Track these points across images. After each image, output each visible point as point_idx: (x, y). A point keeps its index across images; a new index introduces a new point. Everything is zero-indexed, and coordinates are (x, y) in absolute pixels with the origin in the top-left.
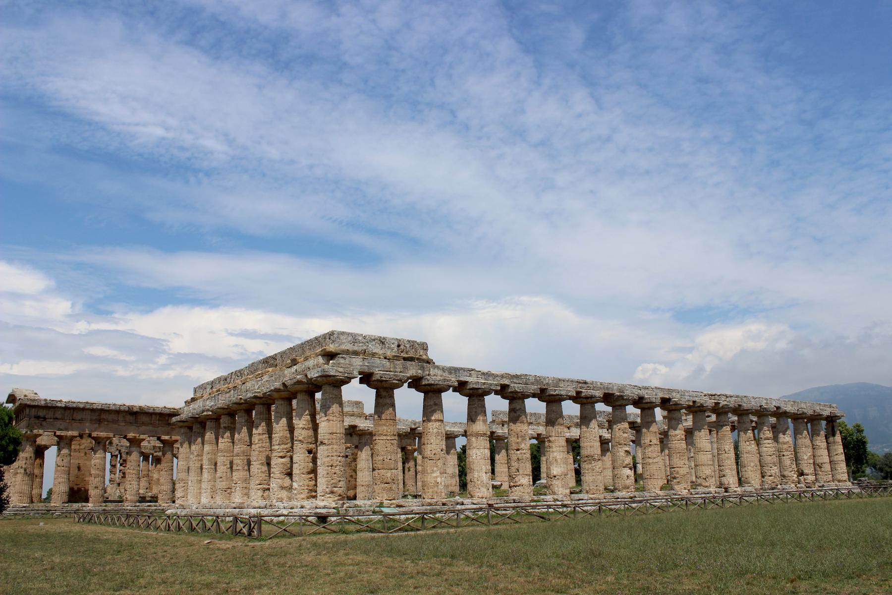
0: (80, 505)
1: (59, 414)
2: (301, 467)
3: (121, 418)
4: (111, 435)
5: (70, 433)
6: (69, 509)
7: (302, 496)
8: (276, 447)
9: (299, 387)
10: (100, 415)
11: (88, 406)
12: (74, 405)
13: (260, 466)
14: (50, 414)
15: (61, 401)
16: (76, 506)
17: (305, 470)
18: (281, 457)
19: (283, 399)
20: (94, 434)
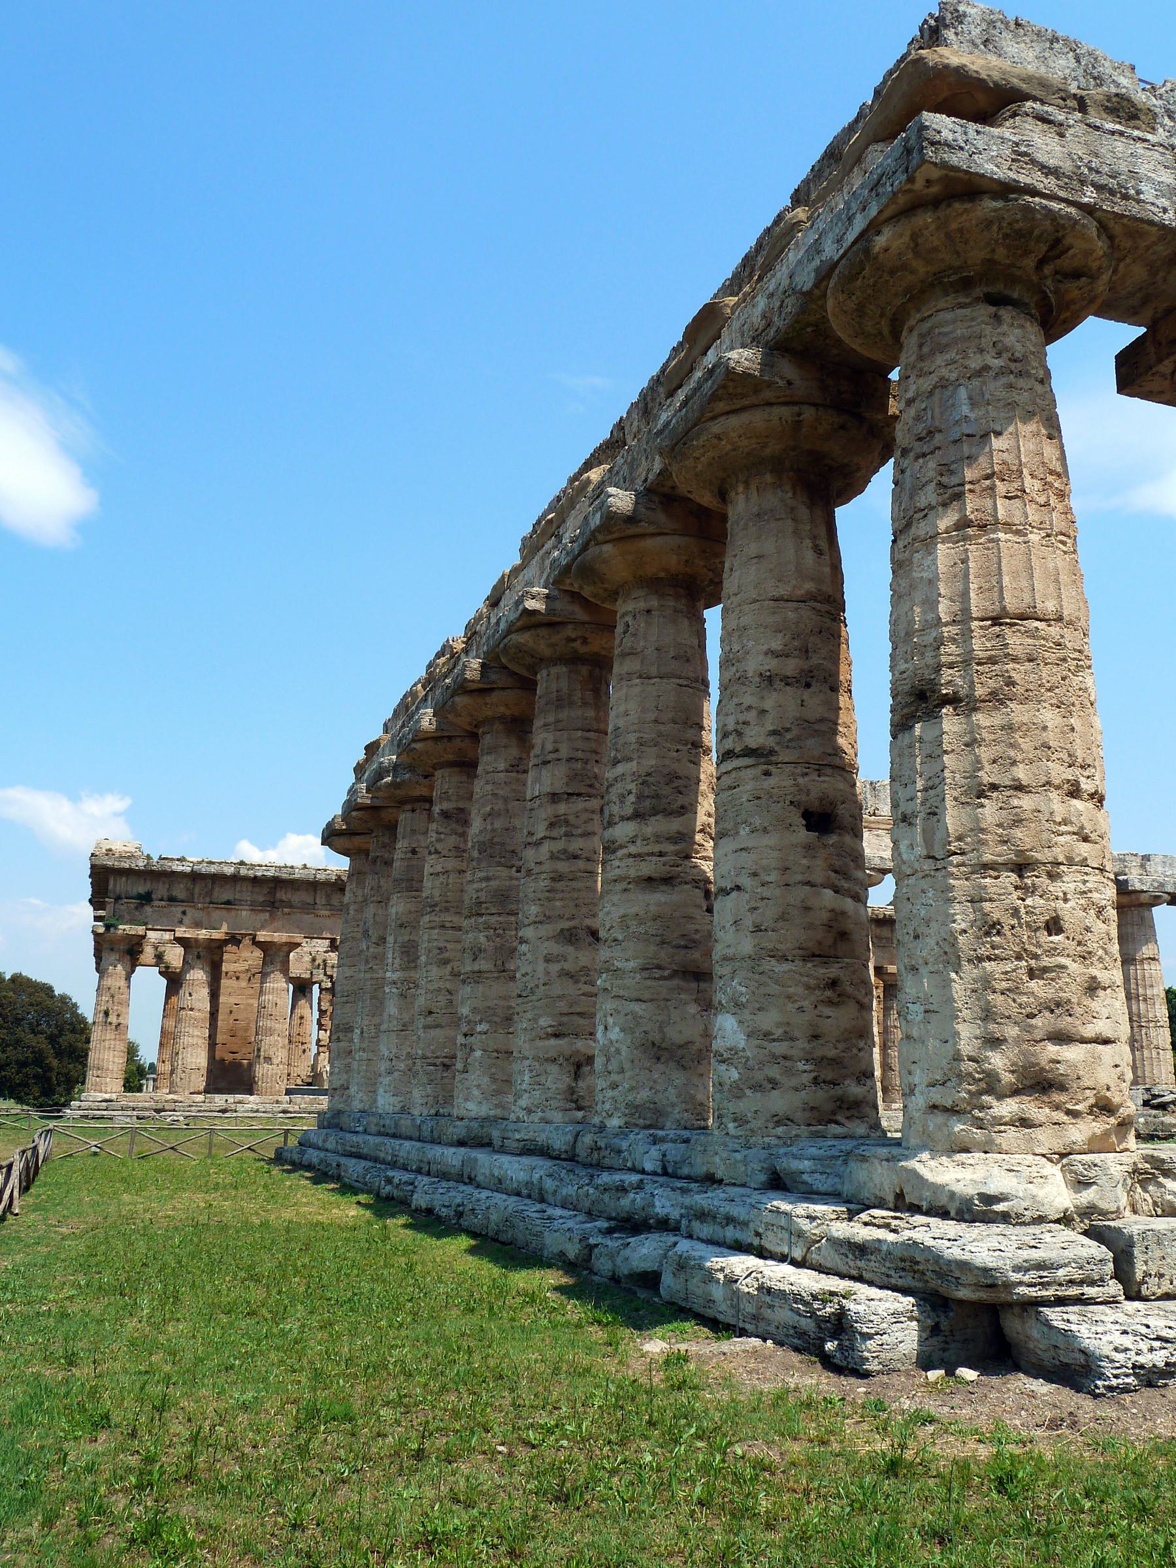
0: (231, 1098)
1: (179, 891)
2: (769, 913)
3: (321, 900)
4: (298, 937)
5: (203, 934)
6: (205, 1107)
7: (778, 1101)
8: (623, 831)
9: (734, 429)
10: (272, 892)
11: (243, 871)
12: (213, 869)
13: (555, 948)
14: (161, 890)
15: (182, 860)
16: (220, 1100)
17: (792, 937)
18: (650, 881)
19: (652, 584)
20: (262, 936)
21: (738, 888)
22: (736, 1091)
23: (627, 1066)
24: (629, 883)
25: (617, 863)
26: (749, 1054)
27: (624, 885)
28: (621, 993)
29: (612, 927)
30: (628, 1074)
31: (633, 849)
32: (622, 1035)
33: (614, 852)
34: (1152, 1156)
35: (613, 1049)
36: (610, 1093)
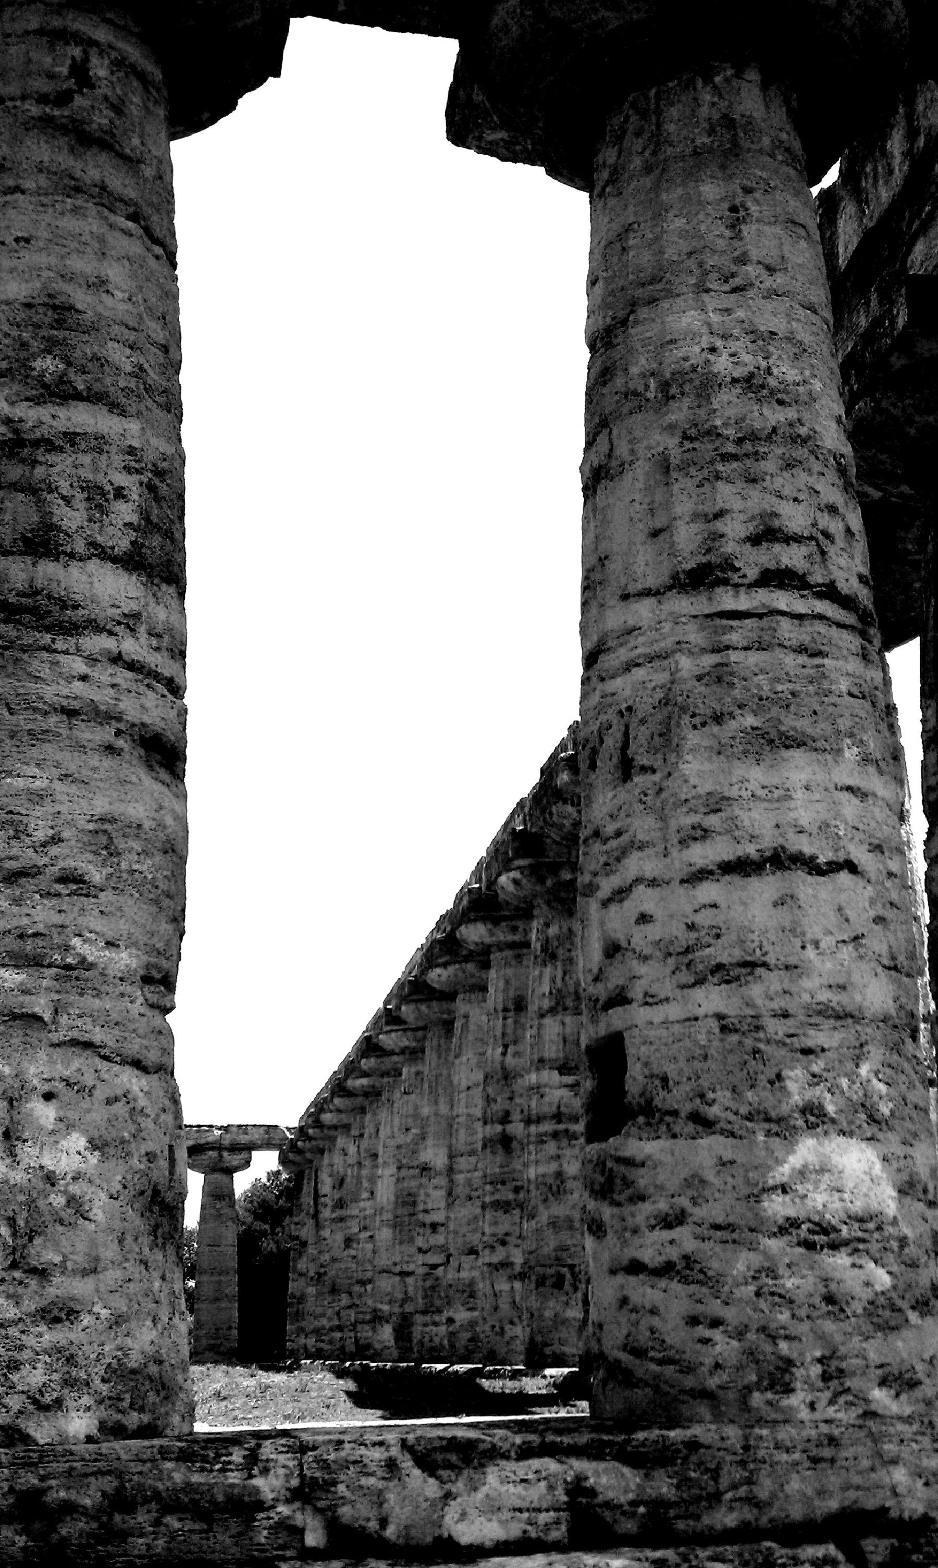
21: (851, 867)
22: (884, 1316)
23: (110, 1252)
24: (118, 733)
25: (79, 666)
26: (907, 1231)
27: (106, 734)
28: (98, 1036)
29: (56, 840)
30: (111, 1276)
31: (131, 647)
32: (94, 1159)
33: (72, 629)
34: (684, 1427)
35: (58, 1200)
36: (49, 1336)
